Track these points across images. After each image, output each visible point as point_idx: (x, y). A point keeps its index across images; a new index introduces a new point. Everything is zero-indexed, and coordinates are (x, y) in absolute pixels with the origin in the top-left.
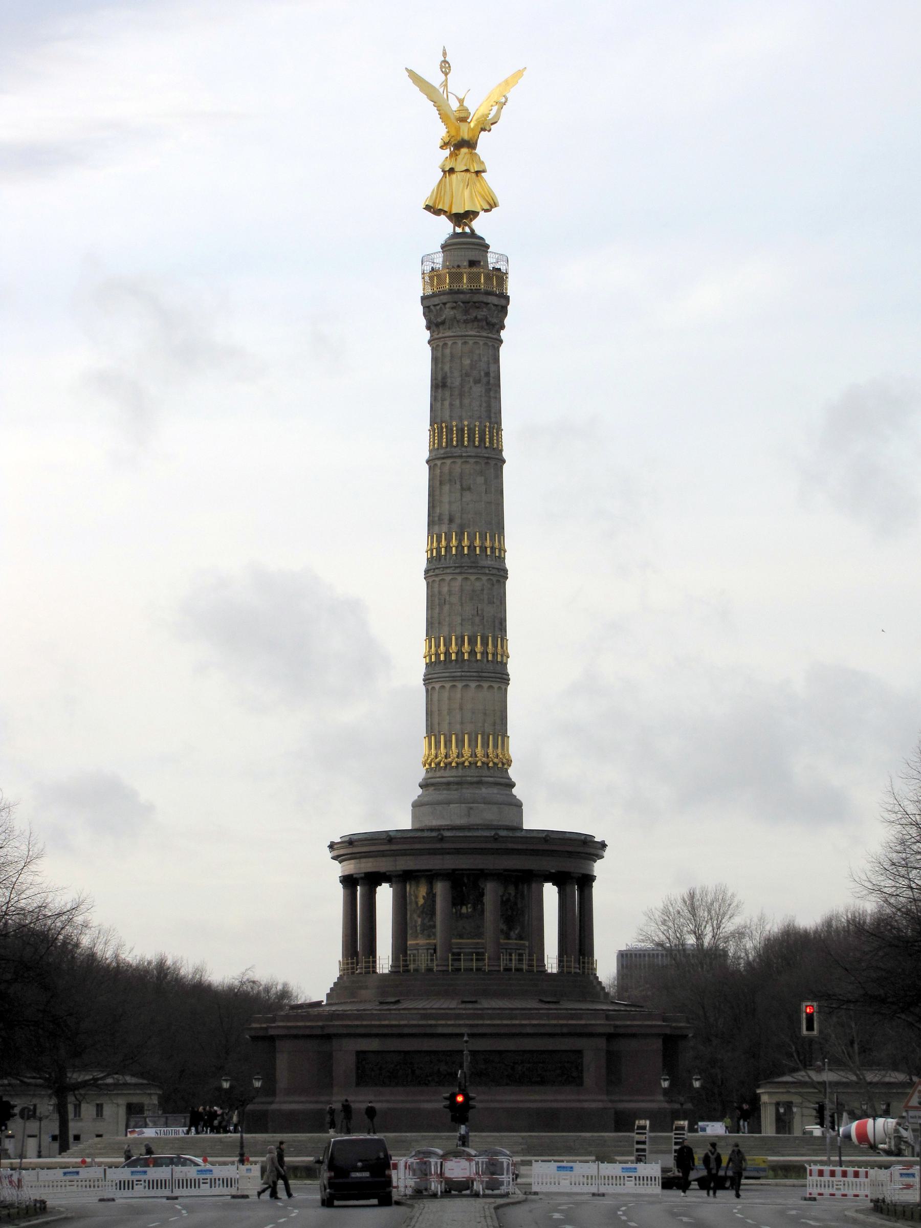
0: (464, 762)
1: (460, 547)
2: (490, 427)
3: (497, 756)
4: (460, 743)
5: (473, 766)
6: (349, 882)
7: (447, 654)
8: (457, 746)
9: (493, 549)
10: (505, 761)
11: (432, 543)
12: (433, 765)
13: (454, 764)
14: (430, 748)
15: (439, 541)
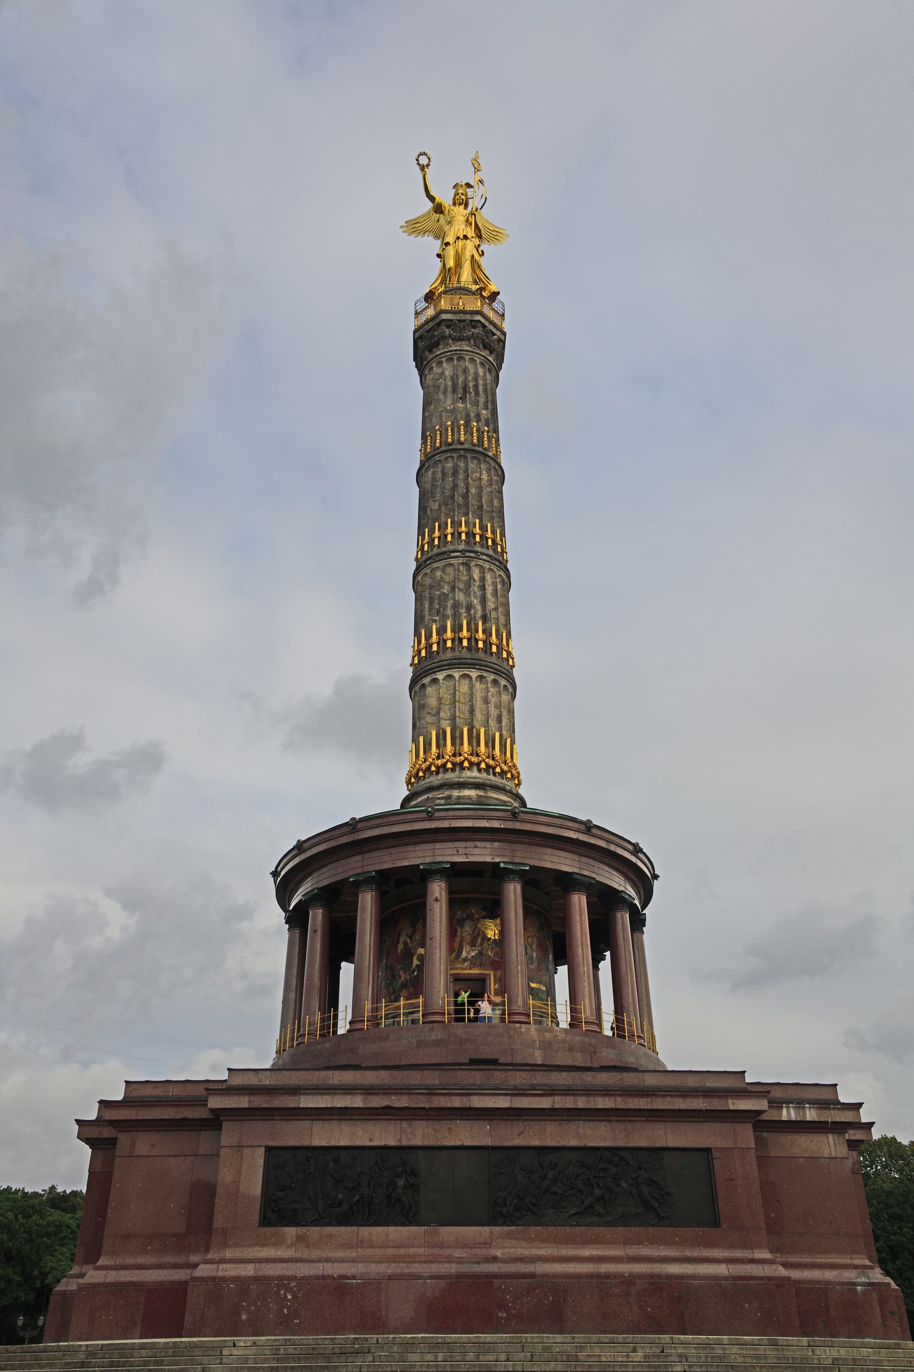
0: (462, 763)
1: (457, 535)
2: (488, 432)
3: (505, 763)
4: (458, 742)
5: (475, 768)
6: (297, 919)
7: (442, 642)
8: (453, 744)
9: (494, 541)
10: (514, 771)
11: (423, 539)
12: (421, 774)
13: (449, 765)
14: (417, 756)
15: (432, 532)
